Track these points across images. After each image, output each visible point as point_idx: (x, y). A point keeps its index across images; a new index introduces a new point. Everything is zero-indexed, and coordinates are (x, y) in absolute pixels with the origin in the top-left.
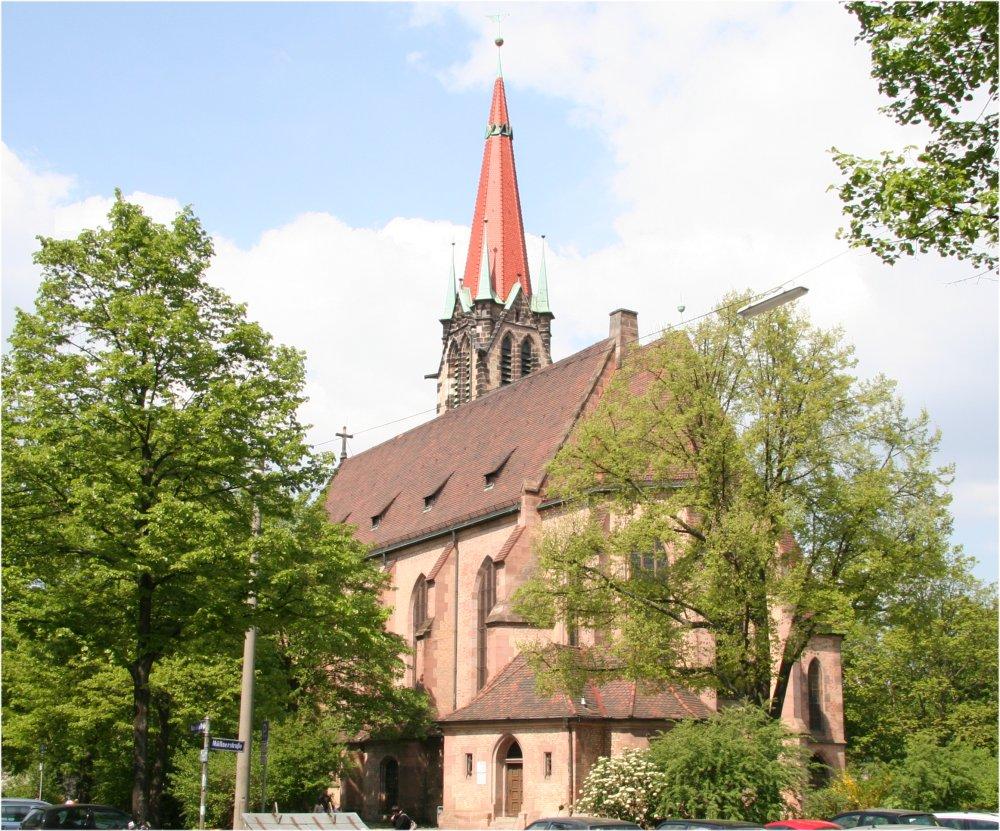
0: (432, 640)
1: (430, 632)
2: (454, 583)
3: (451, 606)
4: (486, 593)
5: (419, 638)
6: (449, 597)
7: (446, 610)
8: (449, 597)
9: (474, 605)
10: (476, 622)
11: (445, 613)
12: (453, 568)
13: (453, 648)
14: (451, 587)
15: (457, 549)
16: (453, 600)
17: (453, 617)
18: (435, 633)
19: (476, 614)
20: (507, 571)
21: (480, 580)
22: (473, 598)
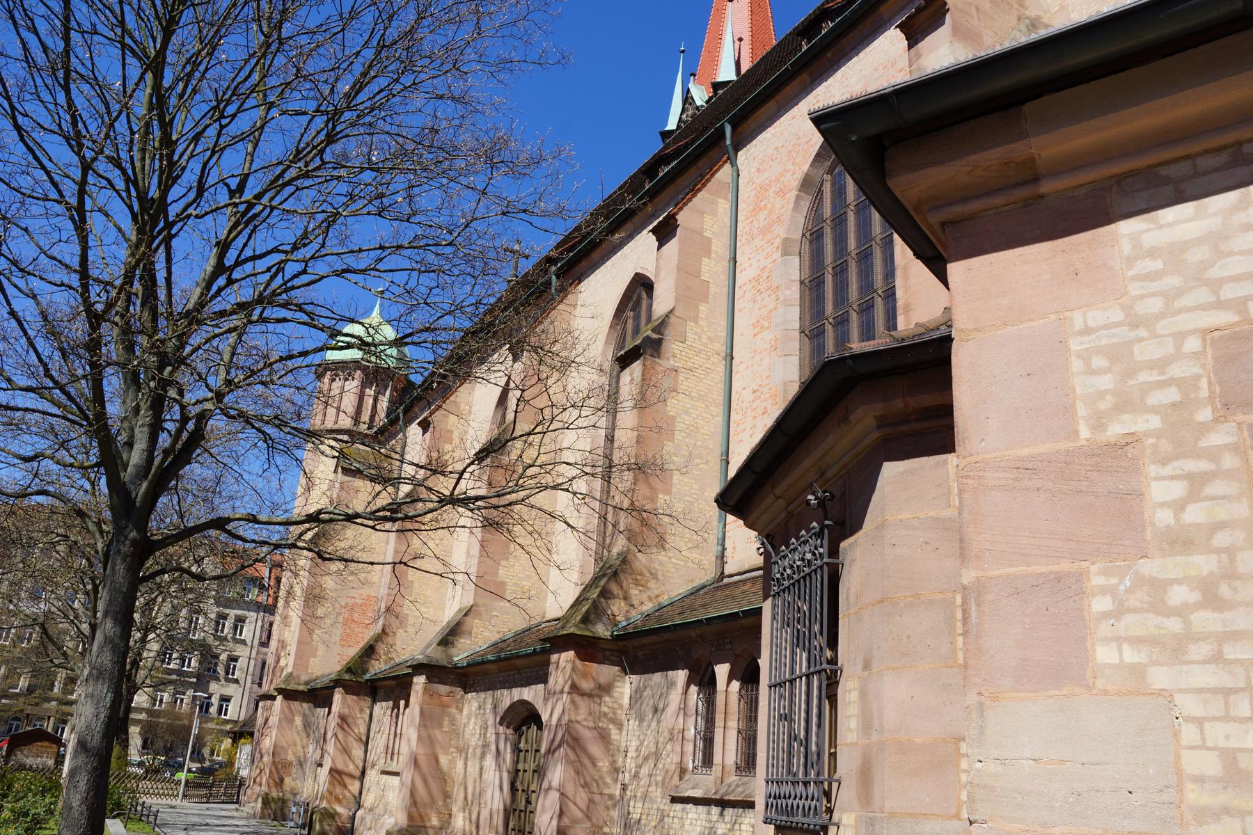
0: (666, 362)
1: (659, 343)
2: (726, 240)
3: (718, 290)
4: (828, 231)
5: (624, 361)
6: (713, 269)
7: (705, 298)
8: (713, 269)
9: (792, 270)
10: (795, 313)
11: (702, 308)
12: (724, 206)
13: (720, 398)
14: (720, 247)
15: (734, 164)
16: (724, 279)
17: (723, 322)
18: (672, 346)
19: (794, 292)
20: (956, 31)
21: (806, 203)
22: (785, 253)
